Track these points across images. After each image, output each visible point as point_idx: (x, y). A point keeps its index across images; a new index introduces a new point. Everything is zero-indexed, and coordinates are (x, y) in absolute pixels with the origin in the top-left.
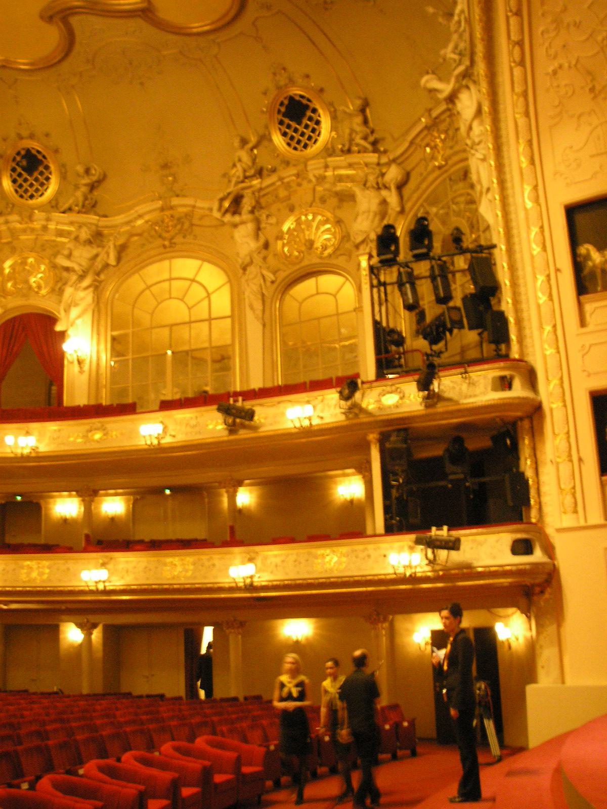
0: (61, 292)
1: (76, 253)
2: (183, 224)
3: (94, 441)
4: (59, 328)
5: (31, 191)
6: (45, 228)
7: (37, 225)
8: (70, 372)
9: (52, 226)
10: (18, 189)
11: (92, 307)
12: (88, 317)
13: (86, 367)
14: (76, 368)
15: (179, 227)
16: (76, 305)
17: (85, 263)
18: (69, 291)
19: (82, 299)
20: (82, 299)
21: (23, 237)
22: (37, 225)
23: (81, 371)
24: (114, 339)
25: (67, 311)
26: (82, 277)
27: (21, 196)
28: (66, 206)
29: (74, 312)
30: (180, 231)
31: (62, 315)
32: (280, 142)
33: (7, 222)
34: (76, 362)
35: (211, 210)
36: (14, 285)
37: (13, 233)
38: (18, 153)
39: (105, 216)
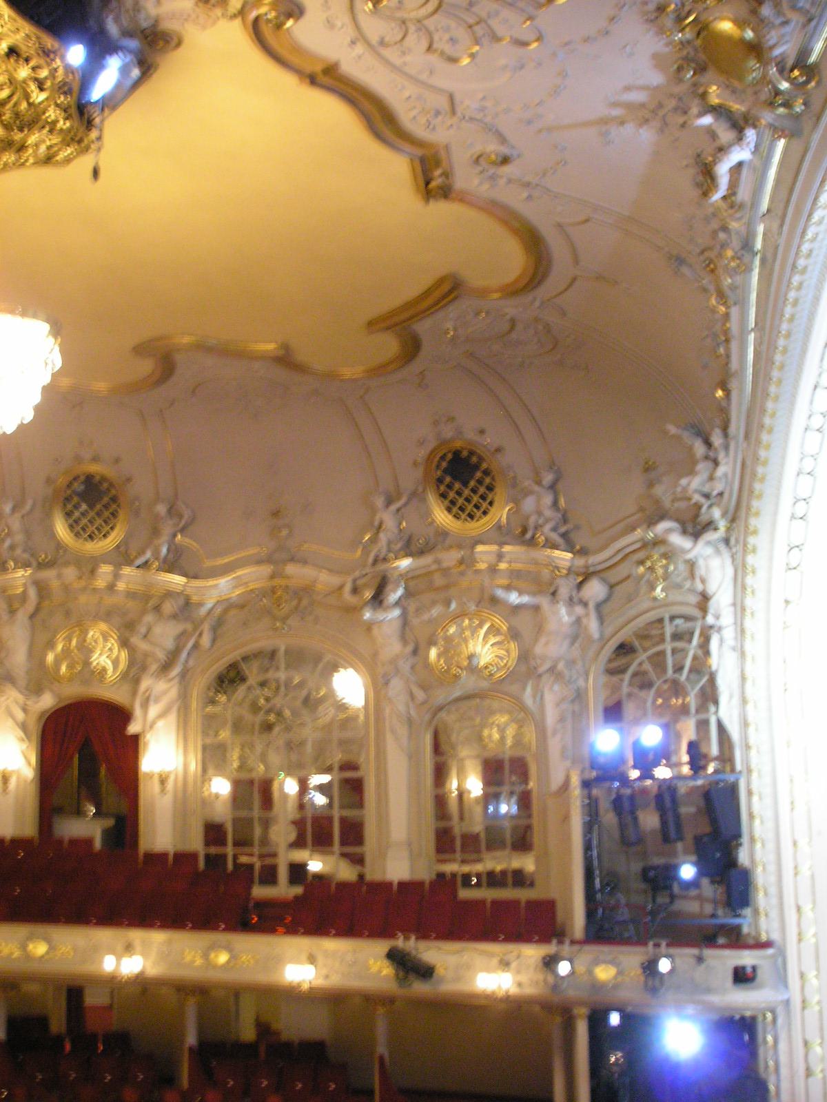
0: (136, 681)
1: (158, 630)
2: (300, 600)
3: (215, 967)
4: (133, 728)
5: (91, 529)
6: (111, 587)
7: (101, 583)
8: (149, 792)
9: (121, 586)
10: (74, 525)
11: (178, 703)
12: (172, 718)
13: (170, 785)
14: (156, 787)
15: (294, 603)
16: (157, 701)
17: (169, 644)
18: (145, 683)
19: (165, 693)
20: (165, 693)
21: (83, 599)
22: (101, 583)
23: (163, 790)
24: (204, 748)
25: (145, 705)
26: (166, 667)
27: (77, 535)
28: (140, 561)
29: (153, 711)
30: (297, 608)
31: (138, 712)
32: (444, 521)
33: (59, 576)
34: (156, 780)
35: (341, 587)
36: (70, 667)
37: (66, 588)
38: (75, 479)
39: (196, 577)
